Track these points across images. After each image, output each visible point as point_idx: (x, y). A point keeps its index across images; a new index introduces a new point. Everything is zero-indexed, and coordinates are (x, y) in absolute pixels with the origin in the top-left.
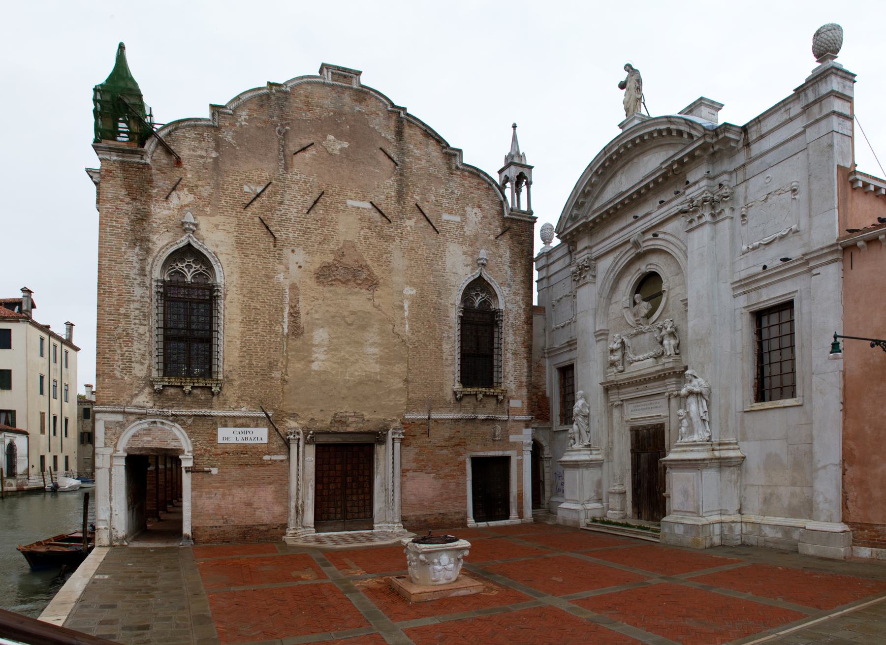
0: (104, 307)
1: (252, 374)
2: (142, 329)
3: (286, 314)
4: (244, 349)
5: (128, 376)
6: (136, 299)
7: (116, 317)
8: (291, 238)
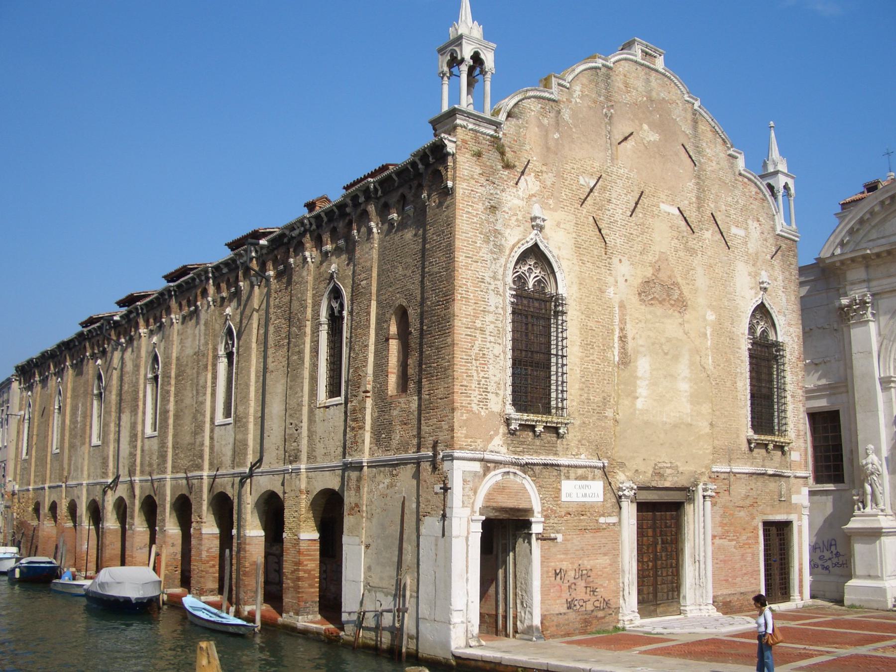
0: (461, 317)
1: (590, 412)
2: (498, 350)
3: (616, 339)
4: (583, 380)
5: (484, 410)
6: (492, 309)
8: (618, 245)
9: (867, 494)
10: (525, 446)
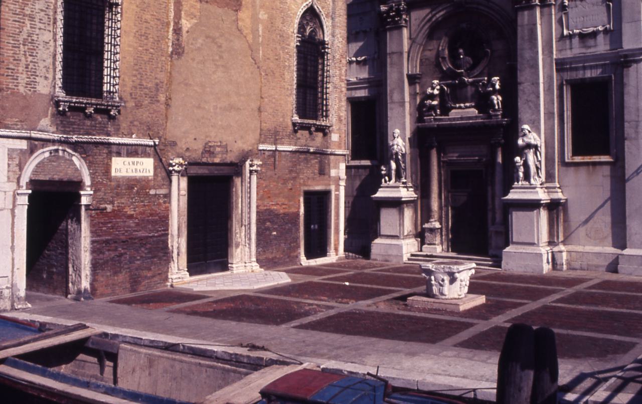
1: (142, 96)
4: (136, 67)
7: (20, 18)
9: (392, 170)
10: (75, 127)
